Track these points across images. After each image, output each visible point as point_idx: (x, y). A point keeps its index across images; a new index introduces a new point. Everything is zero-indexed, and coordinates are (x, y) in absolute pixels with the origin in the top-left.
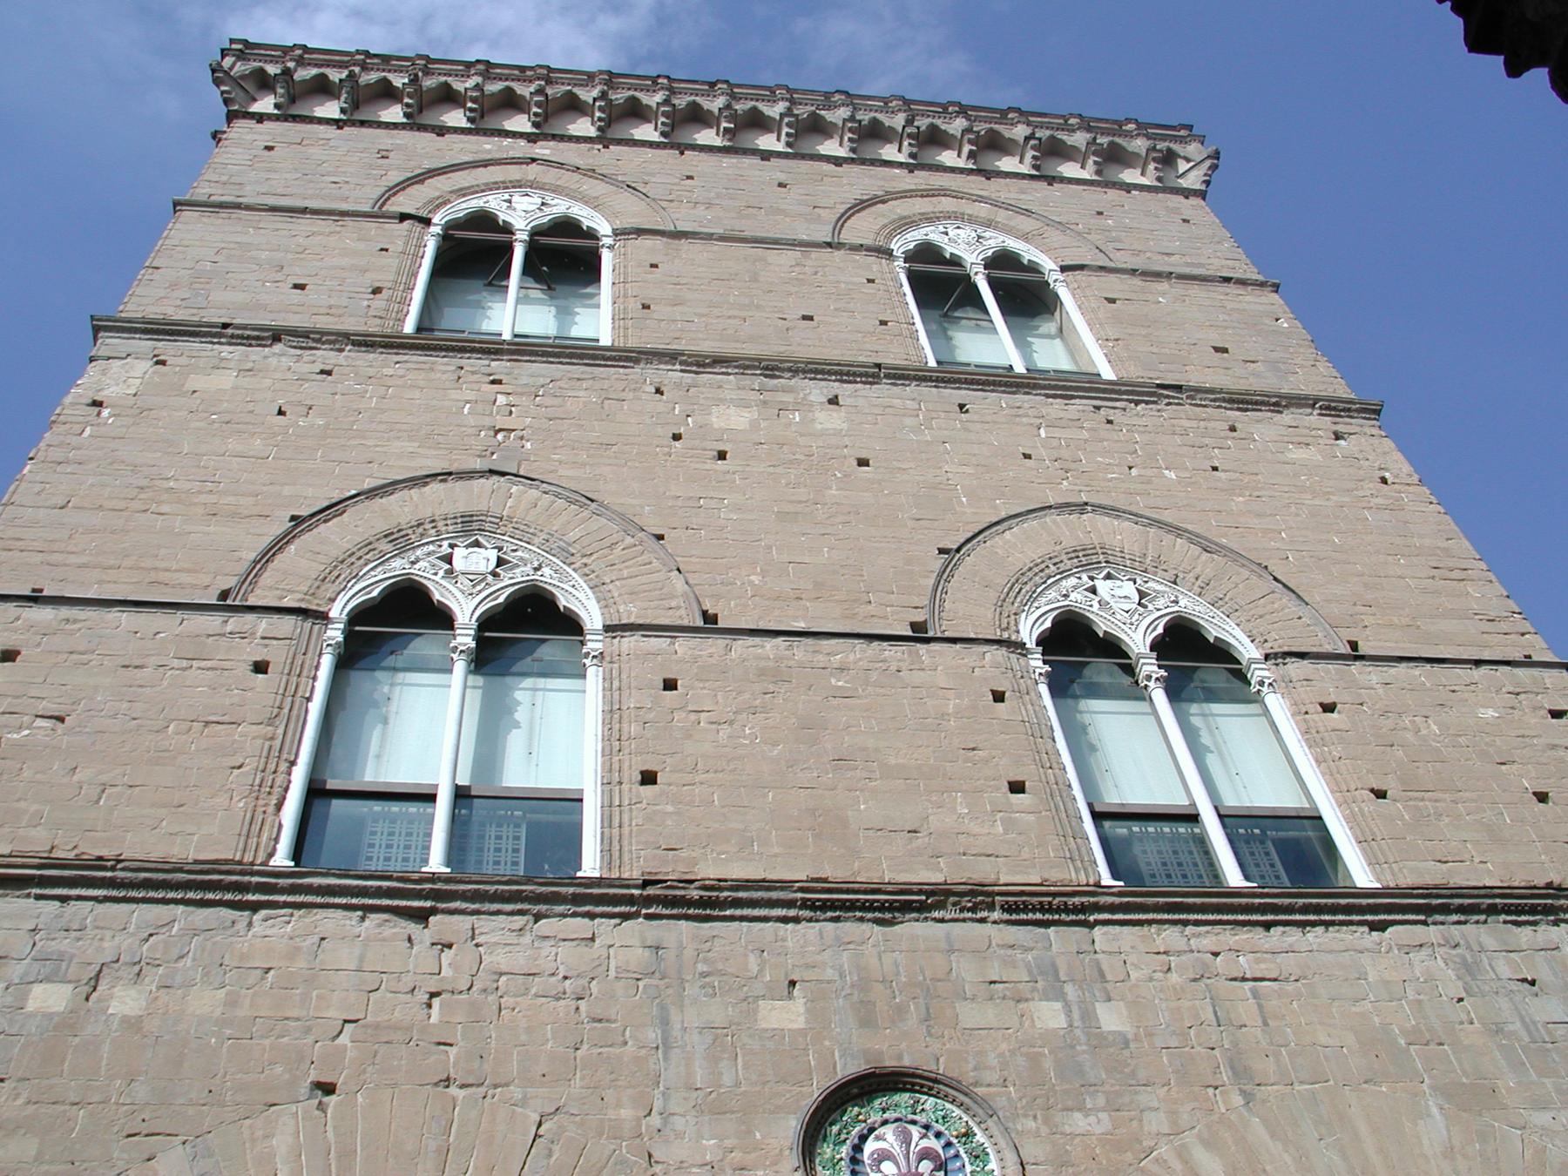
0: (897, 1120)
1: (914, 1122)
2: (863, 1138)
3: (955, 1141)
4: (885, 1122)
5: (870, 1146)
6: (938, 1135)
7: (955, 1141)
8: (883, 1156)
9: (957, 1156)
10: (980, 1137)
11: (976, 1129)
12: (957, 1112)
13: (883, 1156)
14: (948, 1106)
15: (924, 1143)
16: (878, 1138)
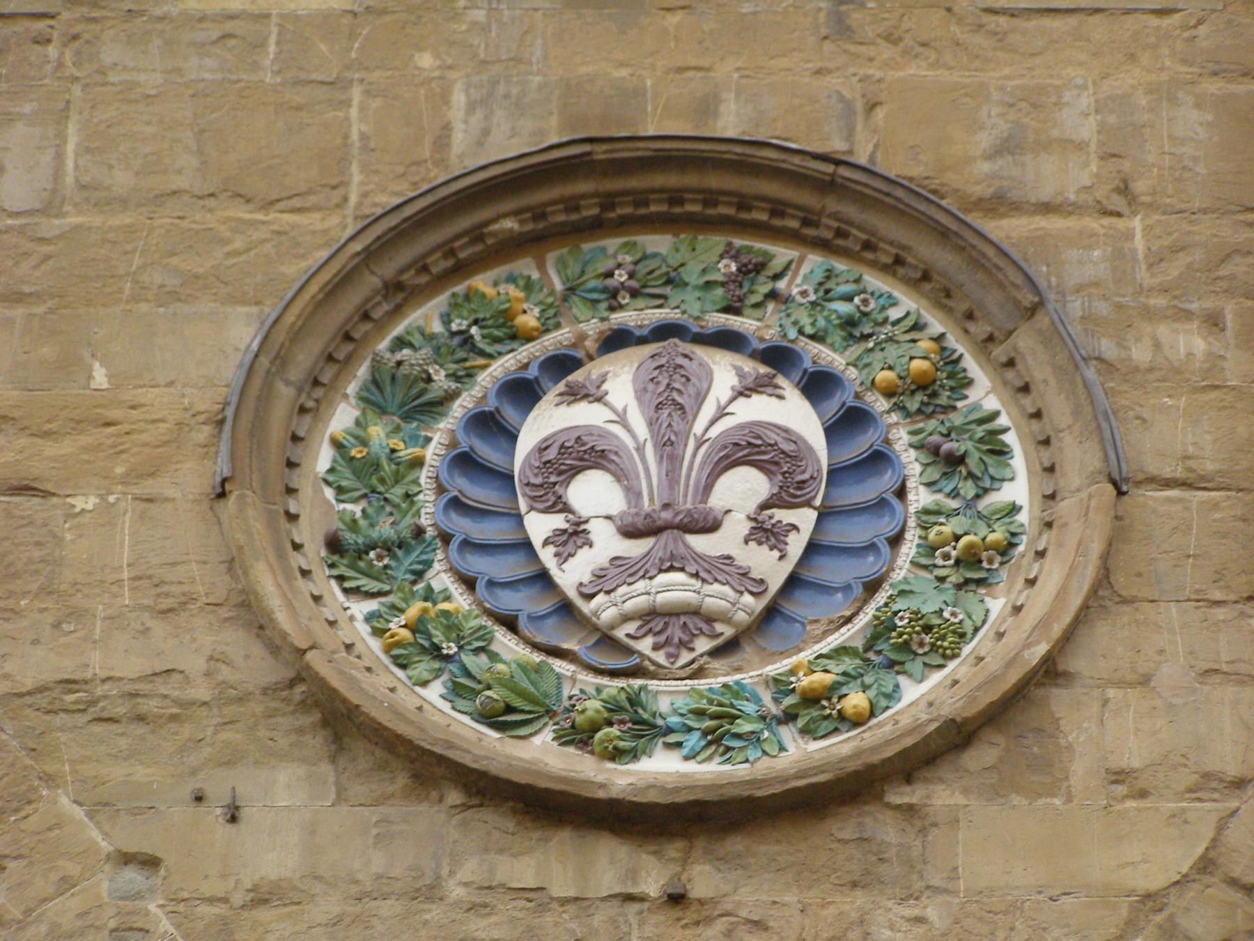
0: (664, 332)
1: (728, 341)
2: (523, 392)
3: (880, 404)
4: (617, 340)
5: (544, 423)
6: (817, 386)
7: (880, 404)
8: (582, 454)
9: (878, 459)
10: (984, 393)
11: (971, 365)
12: (907, 303)
13: (582, 454)
14: (875, 281)
15: (758, 409)
16: (575, 395)
